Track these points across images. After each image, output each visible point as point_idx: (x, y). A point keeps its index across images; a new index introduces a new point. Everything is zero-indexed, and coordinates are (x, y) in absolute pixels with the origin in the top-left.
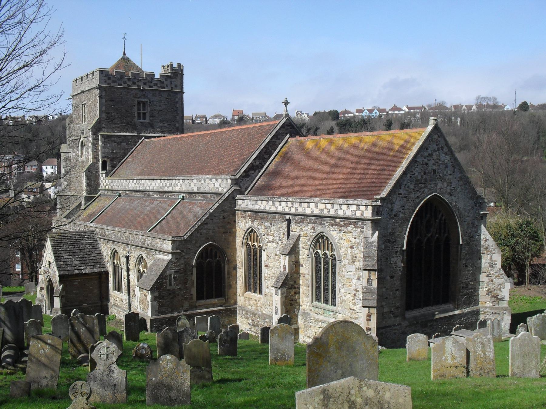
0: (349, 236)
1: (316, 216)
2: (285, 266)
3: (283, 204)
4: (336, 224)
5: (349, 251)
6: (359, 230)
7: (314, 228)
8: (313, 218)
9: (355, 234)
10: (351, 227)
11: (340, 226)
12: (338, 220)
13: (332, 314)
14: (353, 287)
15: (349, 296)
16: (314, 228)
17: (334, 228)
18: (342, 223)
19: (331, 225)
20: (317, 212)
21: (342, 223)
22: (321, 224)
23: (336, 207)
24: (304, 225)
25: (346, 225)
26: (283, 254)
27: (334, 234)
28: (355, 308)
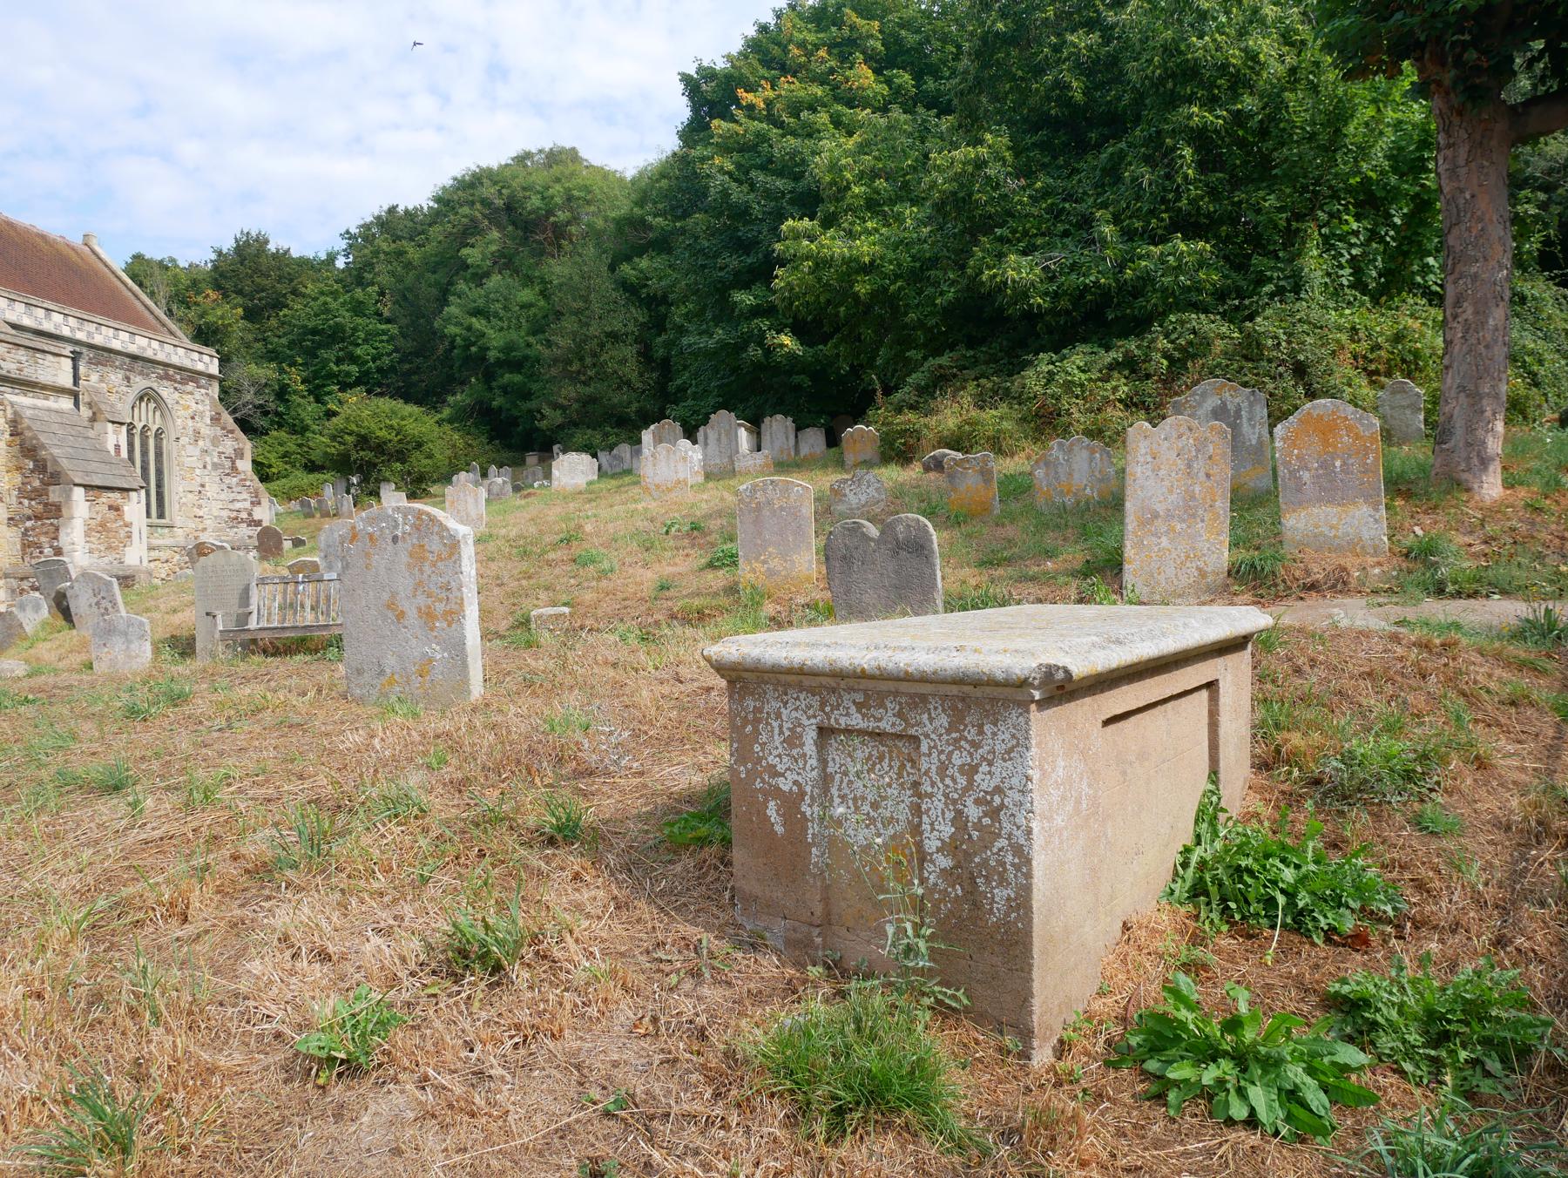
0: (189, 400)
1: (134, 358)
2: (117, 447)
3: (57, 318)
4: (167, 377)
5: (190, 422)
6: (203, 391)
7: (128, 379)
8: (127, 360)
9: (198, 396)
10: (191, 386)
11: (175, 381)
12: (171, 372)
13: (167, 530)
14: (199, 480)
15: (190, 495)
16: (128, 379)
17: (165, 383)
18: (178, 377)
19: (161, 378)
20: (133, 349)
21: (178, 377)
22: (141, 373)
23: (155, 344)
24: (106, 369)
25: (184, 382)
26: (113, 422)
27: (166, 392)
28: (201, 514)
